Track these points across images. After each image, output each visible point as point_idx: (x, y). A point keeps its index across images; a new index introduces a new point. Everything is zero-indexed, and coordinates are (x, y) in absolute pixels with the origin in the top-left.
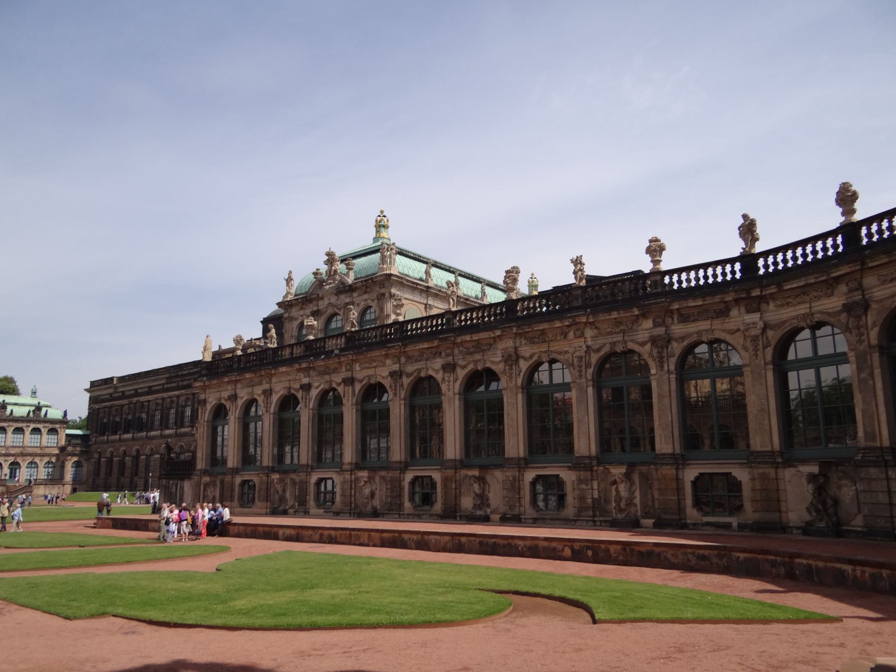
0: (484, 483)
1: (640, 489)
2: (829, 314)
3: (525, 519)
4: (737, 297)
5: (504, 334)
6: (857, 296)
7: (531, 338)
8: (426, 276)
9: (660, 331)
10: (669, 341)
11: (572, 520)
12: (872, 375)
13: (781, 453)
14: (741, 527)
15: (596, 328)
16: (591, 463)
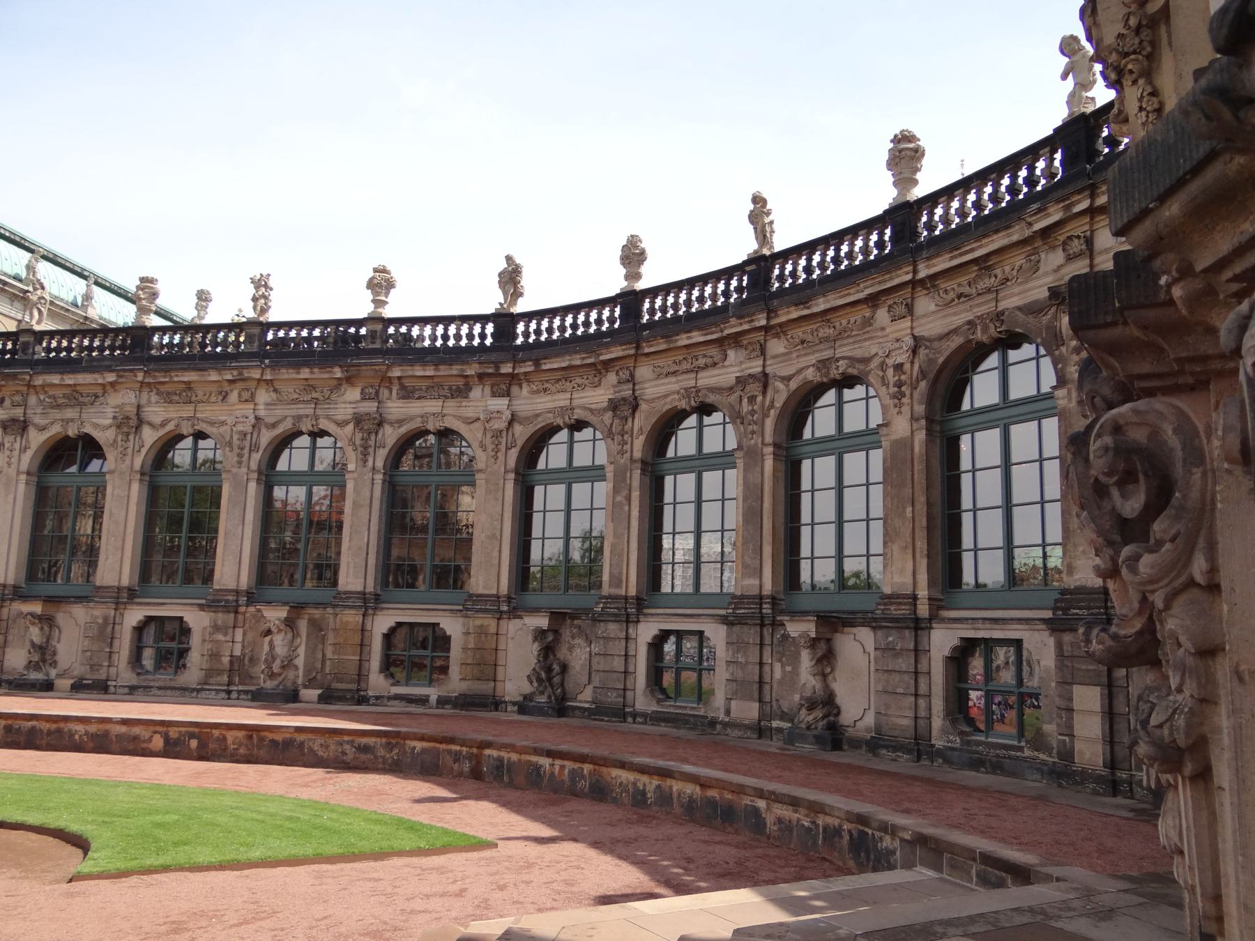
0: (51, 627)
1: (307, 643)
2: (591, 410)
3: (115, 686)
4: (481, 371)
5: (120, 380)
6: (626, 392)
7: (168, 393)
8: (28, 274)
9: (370, 407)
10: (380, 424)
11: (193, 690)
12: (629, 499)
13: (509, 599)
14: (442, 702)
15: (275, 390)
16: (237, 601)
